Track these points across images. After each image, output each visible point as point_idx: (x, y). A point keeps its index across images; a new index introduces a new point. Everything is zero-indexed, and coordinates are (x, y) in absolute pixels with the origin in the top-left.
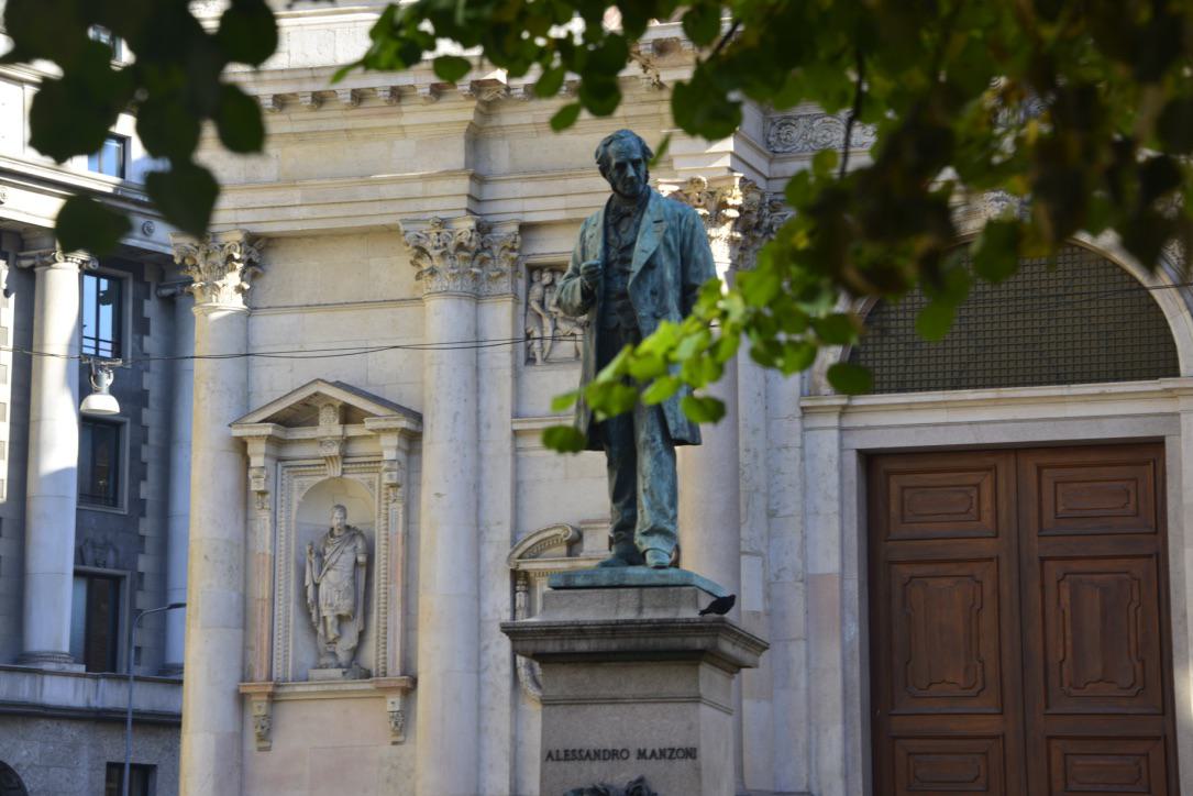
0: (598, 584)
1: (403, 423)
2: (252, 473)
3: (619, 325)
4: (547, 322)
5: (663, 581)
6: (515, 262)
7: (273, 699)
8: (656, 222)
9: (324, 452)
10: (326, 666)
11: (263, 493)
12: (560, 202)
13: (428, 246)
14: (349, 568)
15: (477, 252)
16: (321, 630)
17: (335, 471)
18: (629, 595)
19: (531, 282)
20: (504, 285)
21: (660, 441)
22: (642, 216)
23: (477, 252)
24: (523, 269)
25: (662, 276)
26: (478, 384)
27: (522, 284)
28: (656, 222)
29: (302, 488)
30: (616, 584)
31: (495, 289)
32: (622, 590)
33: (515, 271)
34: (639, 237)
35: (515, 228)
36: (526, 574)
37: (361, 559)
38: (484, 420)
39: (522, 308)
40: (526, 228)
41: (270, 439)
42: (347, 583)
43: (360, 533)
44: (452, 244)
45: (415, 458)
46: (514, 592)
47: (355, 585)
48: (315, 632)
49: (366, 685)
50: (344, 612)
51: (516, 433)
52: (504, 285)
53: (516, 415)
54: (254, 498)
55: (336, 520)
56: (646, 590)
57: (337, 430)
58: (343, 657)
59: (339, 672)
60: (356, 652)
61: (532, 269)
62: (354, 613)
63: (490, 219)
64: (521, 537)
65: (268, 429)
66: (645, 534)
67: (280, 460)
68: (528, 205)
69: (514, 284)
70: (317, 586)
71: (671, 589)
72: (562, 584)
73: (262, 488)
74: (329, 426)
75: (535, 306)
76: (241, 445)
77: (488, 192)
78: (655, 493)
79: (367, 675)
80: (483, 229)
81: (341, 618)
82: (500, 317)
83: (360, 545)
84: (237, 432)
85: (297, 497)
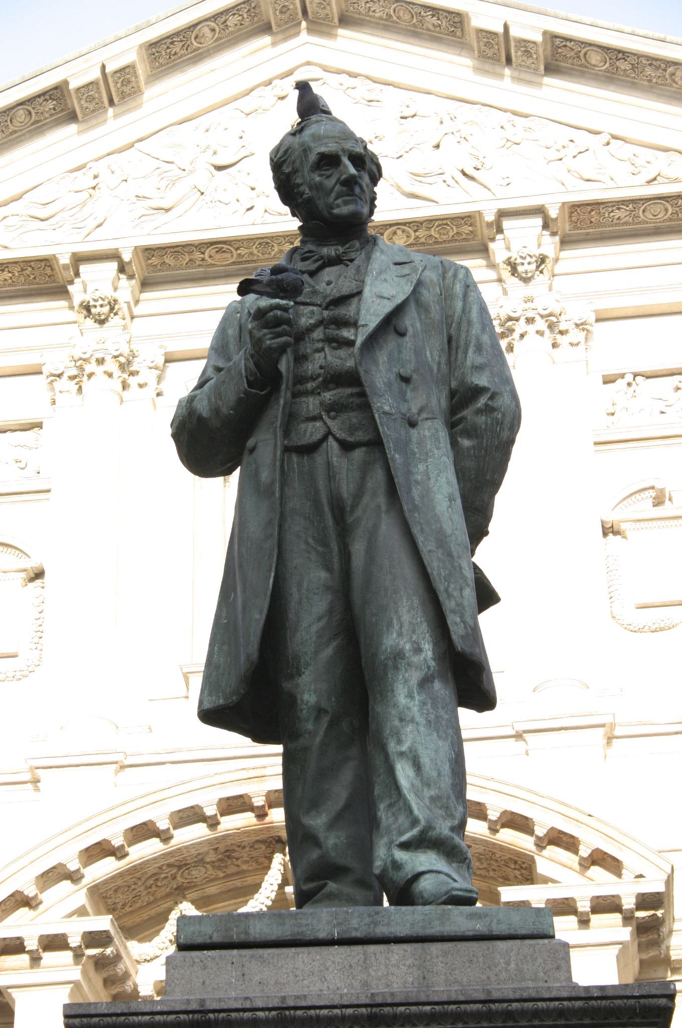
0: (309, 936)
3: (329, 433)
5: (479, 927)
8: (396, 264)
18: (394, 958)
21: (430, 654)
22: (368, 258)
25: (418, 352)
28: (396, 264)
30: (355, 934)
32: (372, 948)
34: (368, 280)
56: (435, 948)
66: (405, 846)
71: (501, 945)
72: (217, 938)
78: (425, 760)
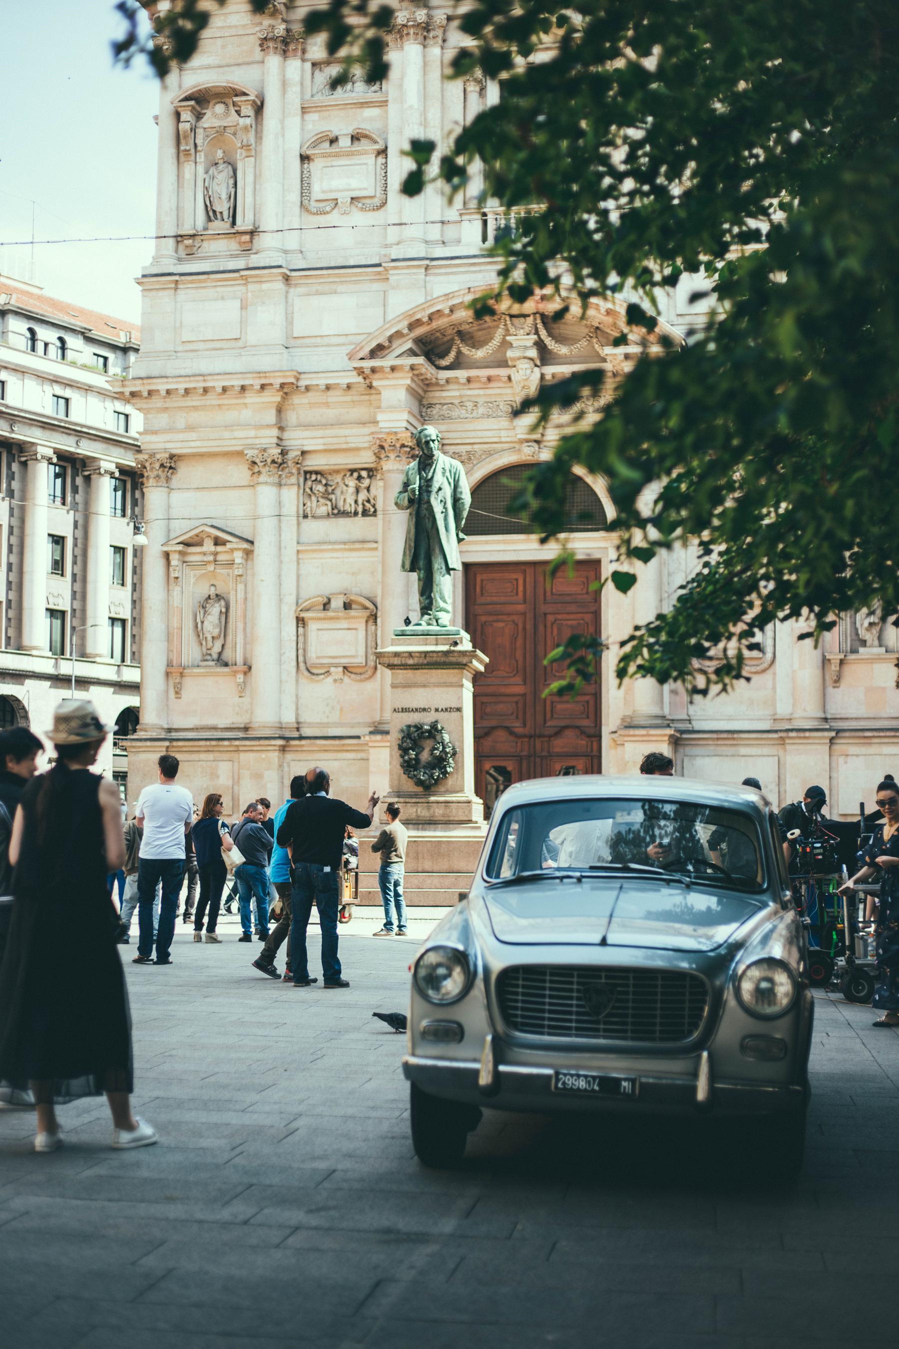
1: (246, 546)
2: (171, 569)
4: (314, 498)
6: (299, 469)
7: (182, 675)
9: (206, 559)
10: (207, 660)
11: (177, 578)
12: (321, 441)
13: (257, 461)
14: (217, 614)
15: (281, 464)
16: (204, 643)
17: (211, 568)
19: (306, 479)
20: (293, 480)
23: (281, 464)
24: (302, 472)
26: (280, 527)
27: (302, 480)
29: (195, 576)
31: (289, 482)
33: (299, 473)
35: (299, 453)
36: (303, 619)
37: (224, 610)
38: (283, 545)
39: (301, 491)
40: (303, 453)
41: (180, 552)
42: (217, 621)
43: (223, 598)
44: (269, 461)
45: (249, 562)
46: (298, 627)
47: (220, 622)
48: (201, 644)
49: (226, 669)
50: (215, 635)
51: (298, 551)
52: (293, 480)
53: (298, 543)
54: (172, 580)
55: (212, 591)
57: (213, 548)
58: (215, 656)
59: (213, 663)
60: (220, 654)
61: (306, 473)
62: (220, 635)
63: (287, 448)
64: (300, 601)
65: (180, 547)
67: (184, 562)
68: (305, 442)
69: (298, 479)
70: (202, 622)
73: (176, 576)
74: (209, 546)
75: (308, 490)
76: (167, 555)
77: (286, 435)
79: (226, 665)
80: (283, 453)
81: (213, 638)
82: (291, 496)
83: (223, 603)
84: (166, 549)
85: (192, 580)
